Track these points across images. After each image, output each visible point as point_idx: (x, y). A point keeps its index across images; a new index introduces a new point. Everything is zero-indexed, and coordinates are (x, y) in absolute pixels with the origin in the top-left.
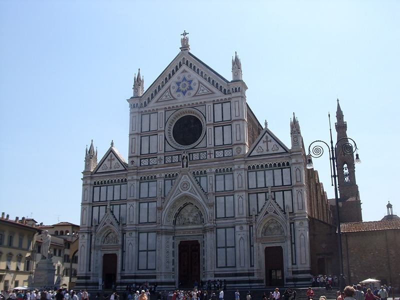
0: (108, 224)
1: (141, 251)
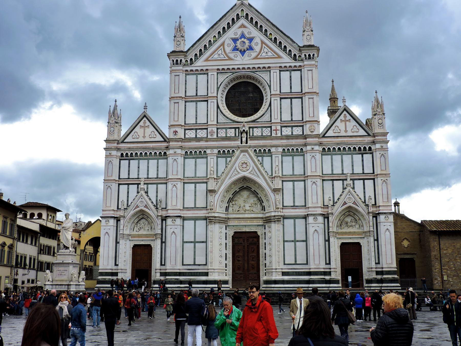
1: (187, 242)
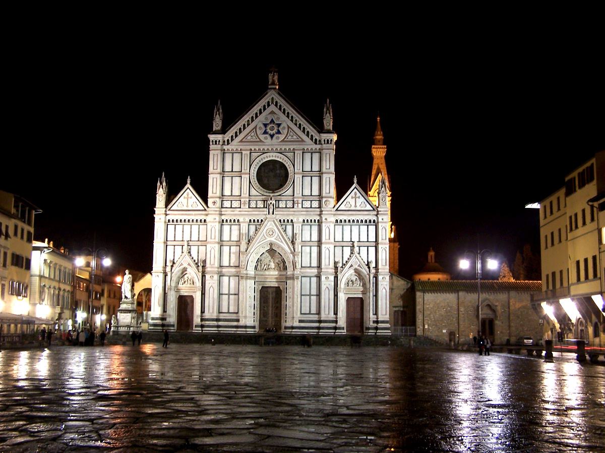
0: (185, 265)
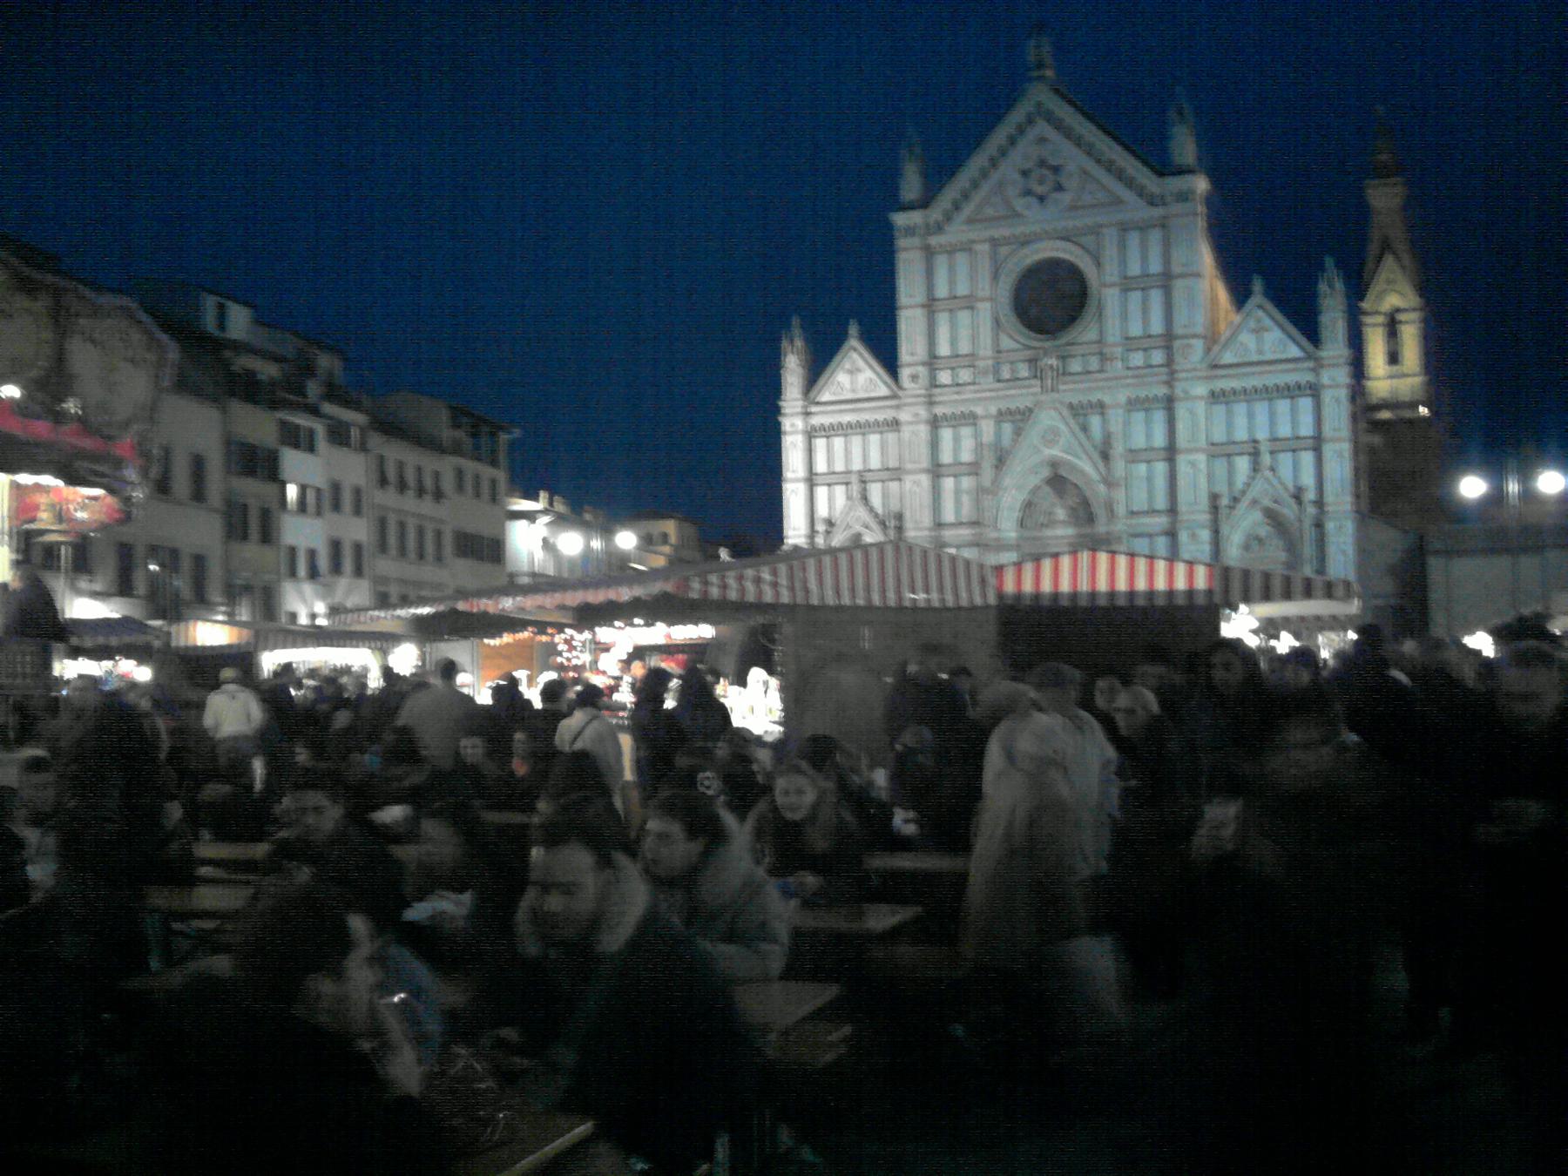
0: (858, 528)
